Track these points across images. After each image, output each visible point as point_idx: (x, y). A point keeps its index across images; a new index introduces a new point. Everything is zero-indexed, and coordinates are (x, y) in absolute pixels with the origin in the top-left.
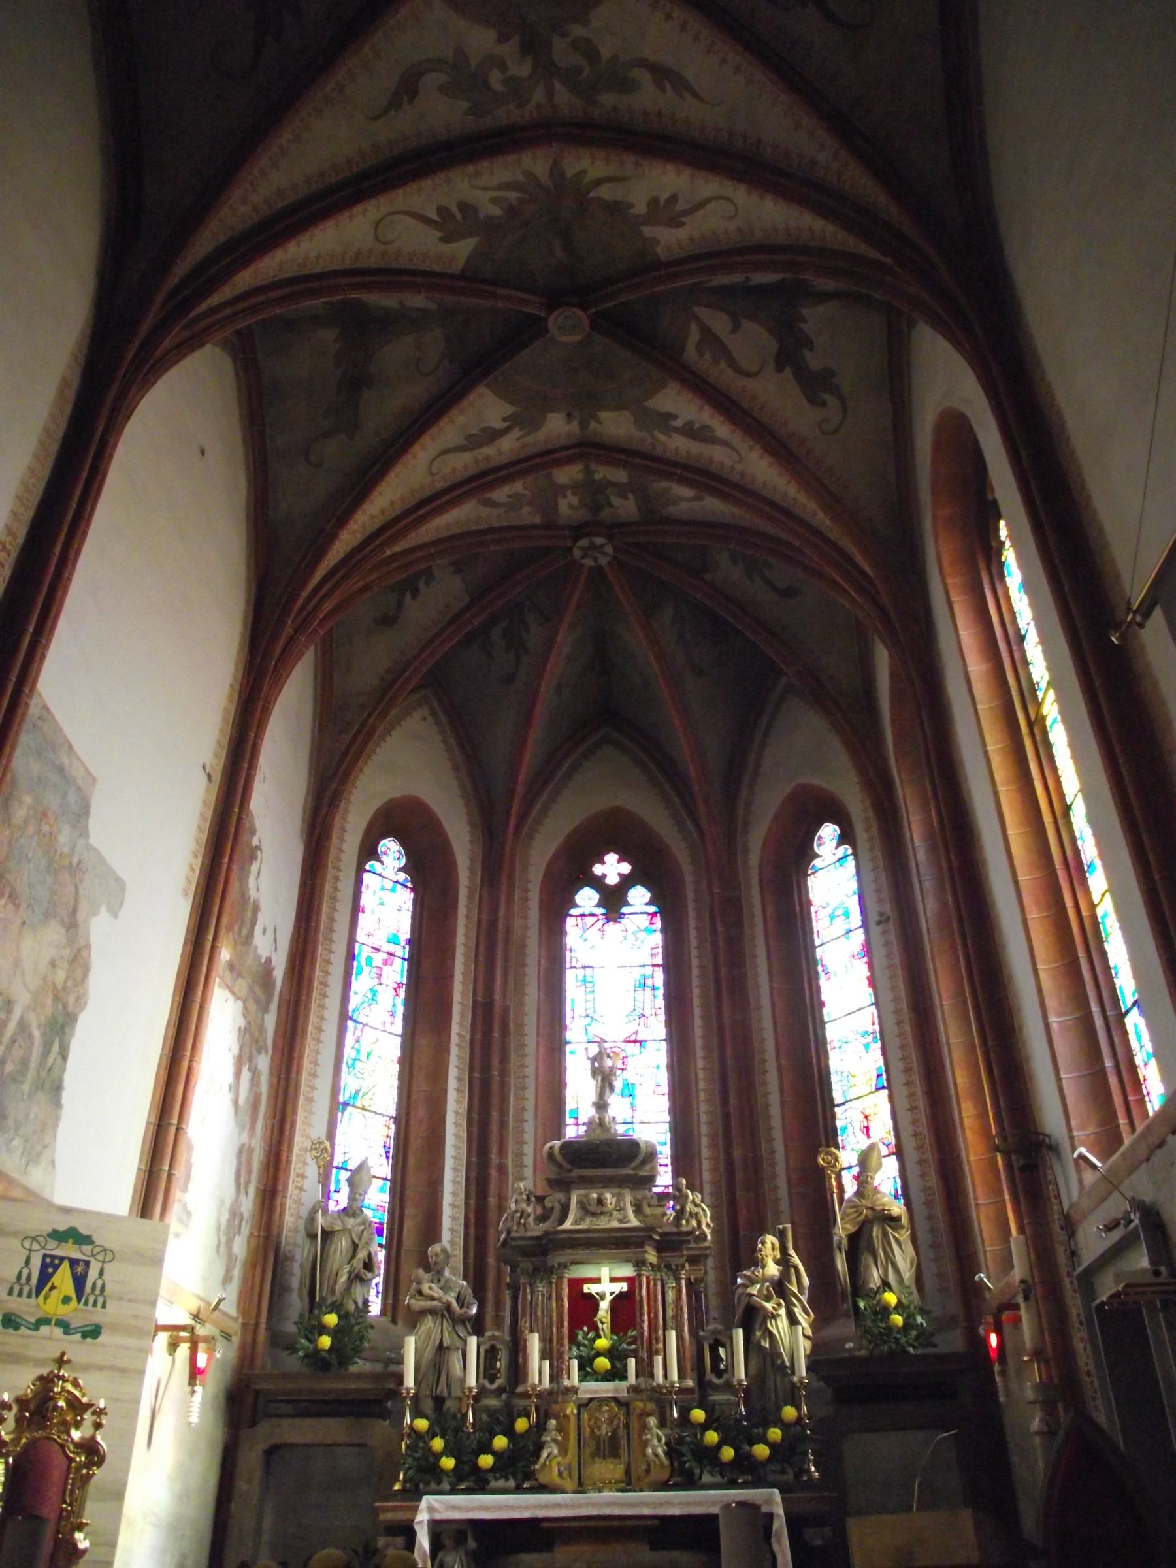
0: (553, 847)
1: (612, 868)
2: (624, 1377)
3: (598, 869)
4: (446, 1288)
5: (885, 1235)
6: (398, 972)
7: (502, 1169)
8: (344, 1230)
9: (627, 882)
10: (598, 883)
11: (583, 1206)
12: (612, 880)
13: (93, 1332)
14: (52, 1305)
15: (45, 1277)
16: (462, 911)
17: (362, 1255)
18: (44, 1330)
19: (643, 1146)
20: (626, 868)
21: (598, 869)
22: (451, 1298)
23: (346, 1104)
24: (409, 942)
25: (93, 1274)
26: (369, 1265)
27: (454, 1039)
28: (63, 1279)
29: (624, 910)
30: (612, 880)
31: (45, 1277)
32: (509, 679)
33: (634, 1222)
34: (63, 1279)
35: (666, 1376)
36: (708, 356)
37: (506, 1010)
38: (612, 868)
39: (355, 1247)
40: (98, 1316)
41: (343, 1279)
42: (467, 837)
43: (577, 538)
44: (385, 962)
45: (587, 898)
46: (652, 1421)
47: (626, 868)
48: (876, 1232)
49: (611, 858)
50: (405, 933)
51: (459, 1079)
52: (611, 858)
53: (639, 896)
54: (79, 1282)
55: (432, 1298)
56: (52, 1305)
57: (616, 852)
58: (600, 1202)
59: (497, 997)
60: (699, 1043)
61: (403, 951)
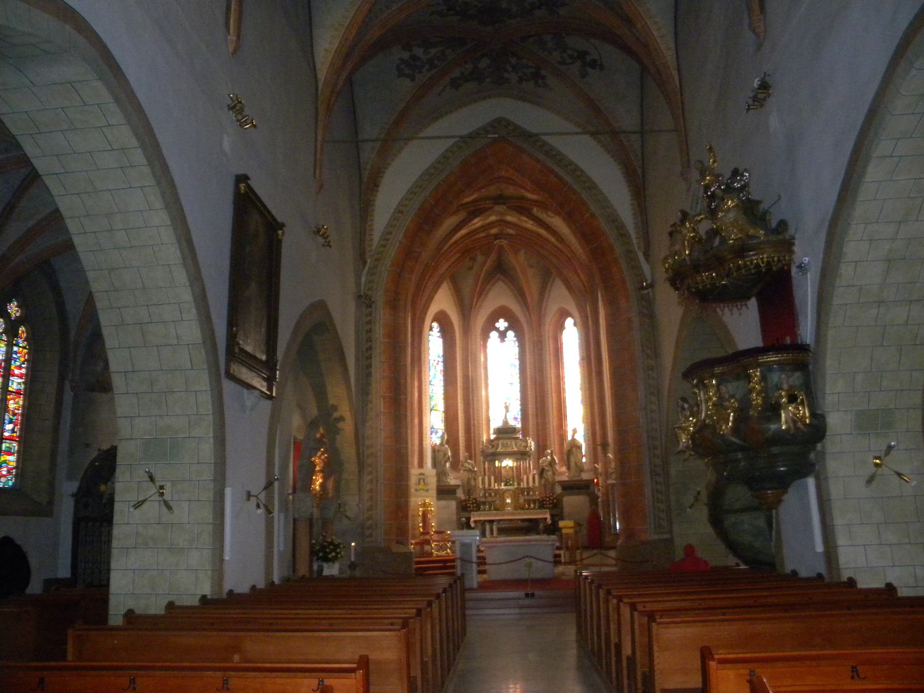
0: (484, 319)
1: (502, 324)
2: (514, 486)
3: (497, 325)
4: (469, 463)
5: (577, 450)
6: (441, 367)
7: (474, 425)
8: (442, 450)
9: (507, 329)
10: (497, 330)
11: (503, 445)
12: (502, 329)
13: (427, 491)
14: (421, 487)
15: (419, 482)
16: (458, 345)
17: (447, 457)
18: (421, 491)
19: (517, 429)
20: (506, 324)
21: (497, 325)
22: (470, 467)
23: (431, 410)
24: (443, 356)
25: (426, 481)
26: (449, 459)
27: (459, 388)
28: (422, 482)
29: (505, 339)
30: (502, 329)
31: (419, 482)
32: (471, 268)
33: (516, 449)
34: (422, 482)
35: (523, 485)
36: (540, 213)
37: (472, 376)
38: (502, 324)
39: (445, 455)
40: (427, 487)
41: (443, 462)
42: (458, 319)
43: (496, 239)
44: (438, 364)
45: (494, 335)
46: (520, 495)
47: (506, 324)
48: (574, 449)
49: (501, 321)
50: (441, 353)
51: (461, 399)
52: (501, 321)
53: (511, 334)
54: (424, 481)
55: (466, 467)
56: (421, 487)
57: (502, 318)
58: (507, 443)
59: (470, 373)
60: (529, 386)
61: (441, 359)
